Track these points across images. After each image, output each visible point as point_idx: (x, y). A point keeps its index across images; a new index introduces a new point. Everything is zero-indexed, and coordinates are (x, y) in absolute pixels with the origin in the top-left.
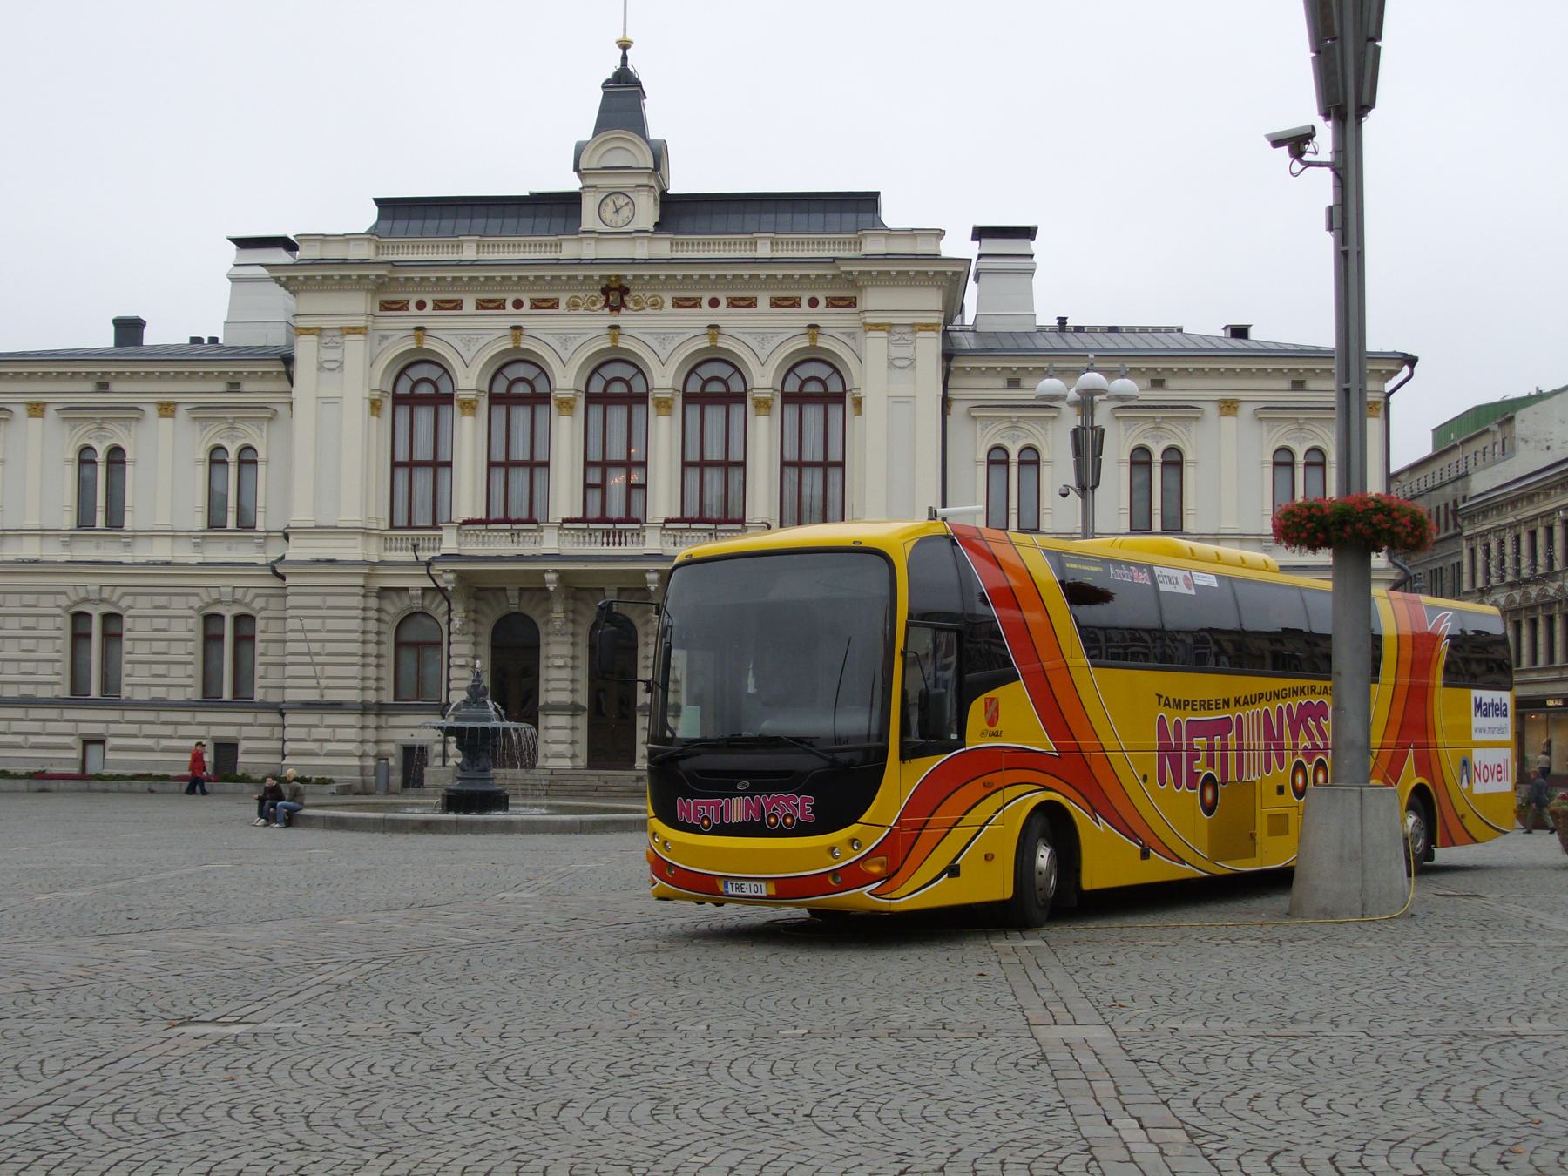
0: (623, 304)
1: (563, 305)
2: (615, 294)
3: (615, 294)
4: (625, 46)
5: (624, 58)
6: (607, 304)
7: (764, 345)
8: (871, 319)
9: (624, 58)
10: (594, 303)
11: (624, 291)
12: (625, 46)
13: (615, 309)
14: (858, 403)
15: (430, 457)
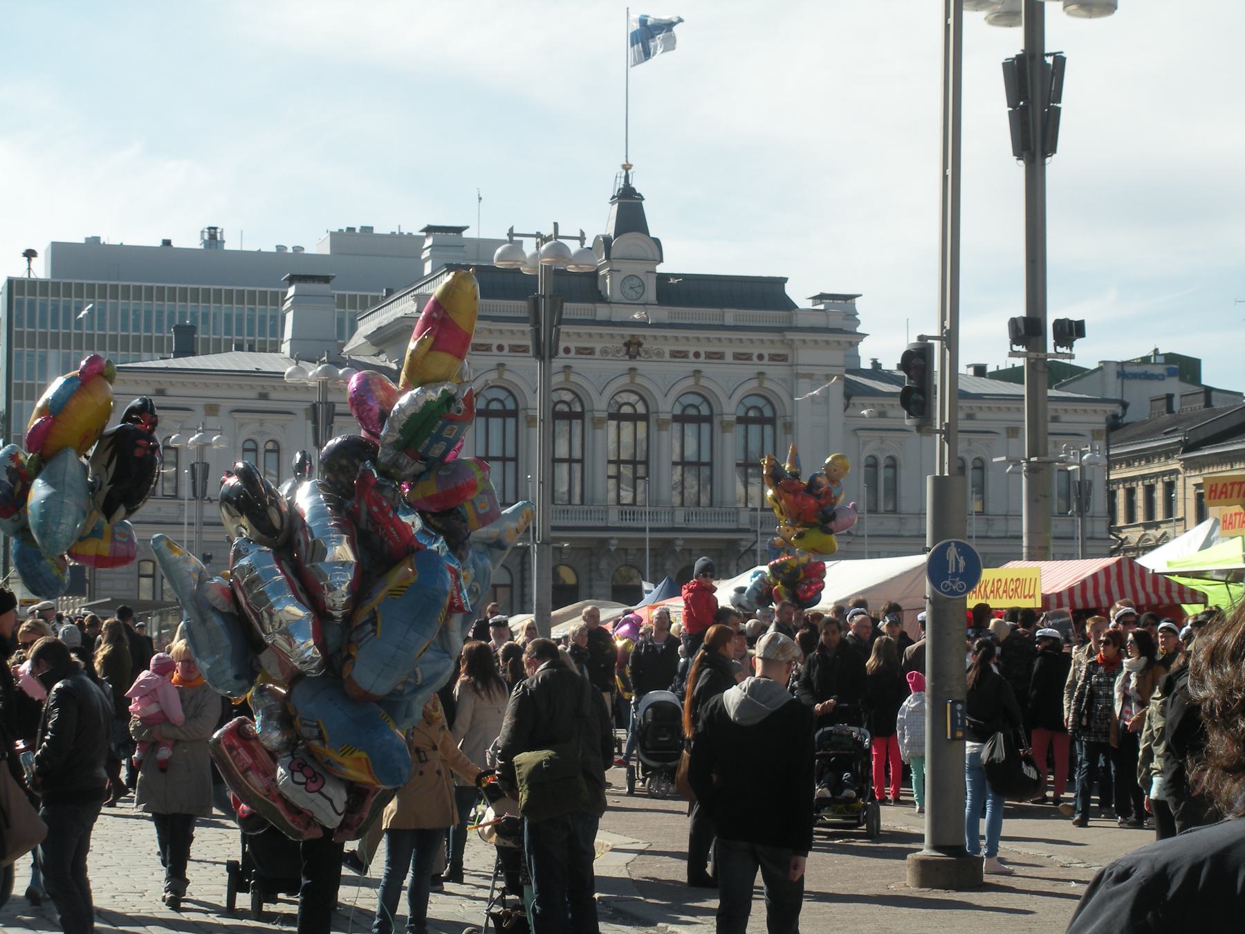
0: (639, 354)
1: (597, 351)
2: (633, 348)
3: (633, 348)
4: (627, 167)
5: (627, 177)
6: (628, 353)
7: (730, 384)
8: (801, 370)
9: (627, 177)
10: (618, 351)
11: (640, 344)
12: (627, 167)
13: (632, 357)
14: (789, 427)
15: (499, 454)
